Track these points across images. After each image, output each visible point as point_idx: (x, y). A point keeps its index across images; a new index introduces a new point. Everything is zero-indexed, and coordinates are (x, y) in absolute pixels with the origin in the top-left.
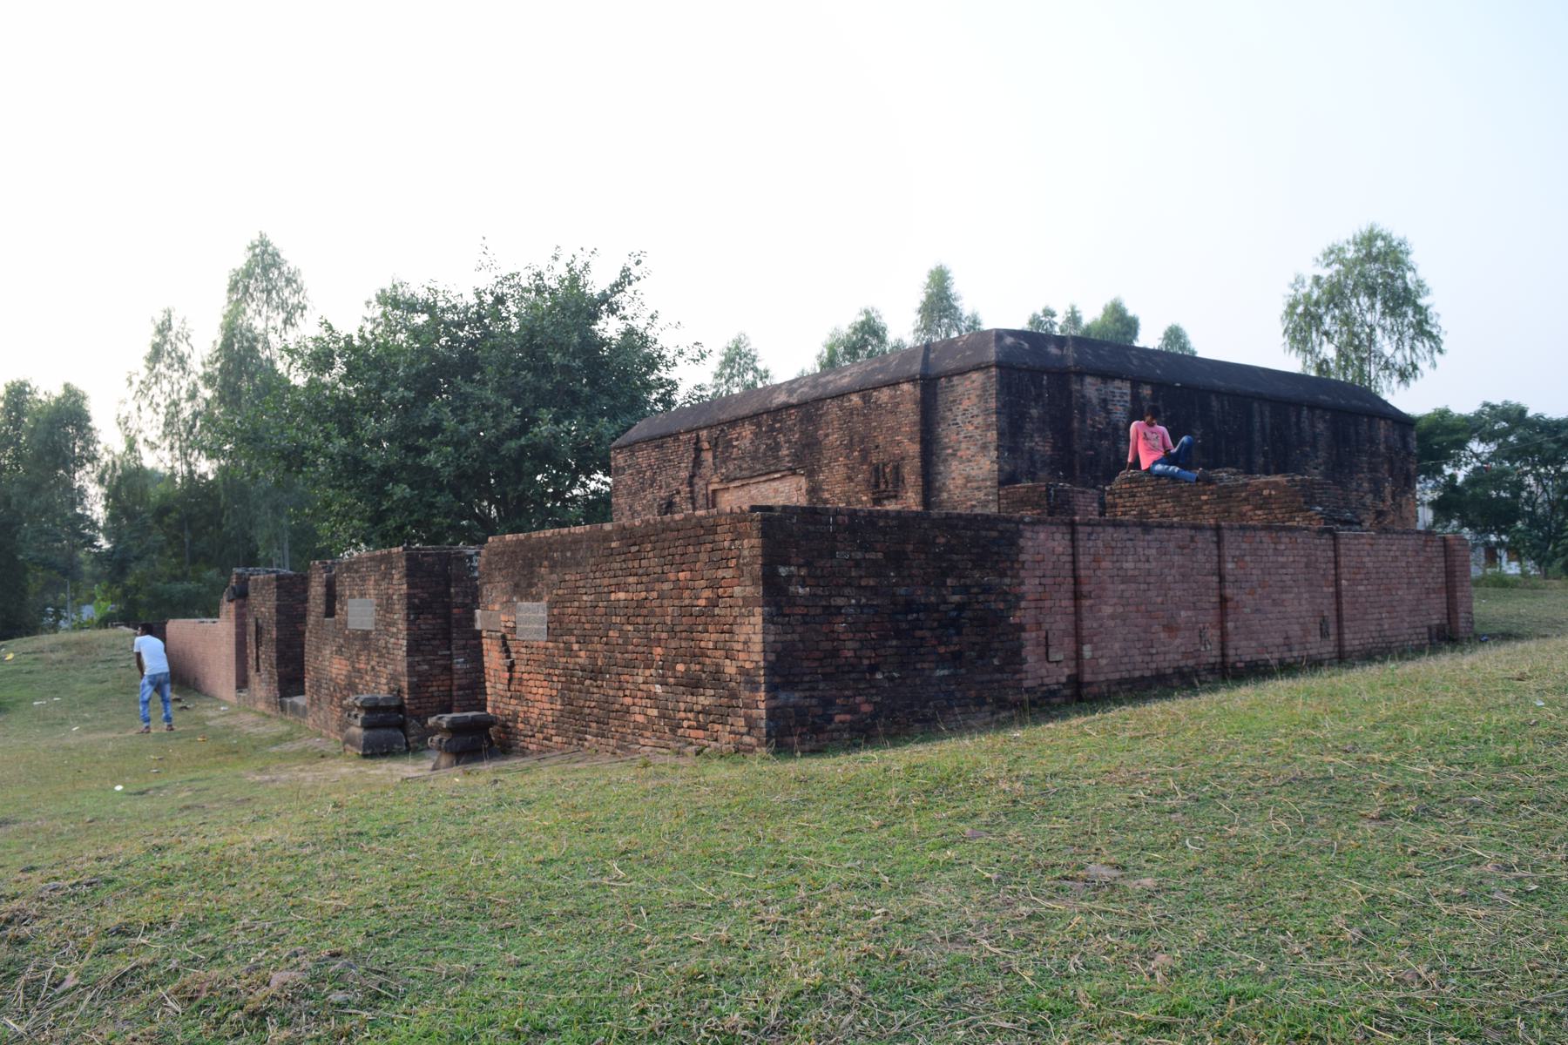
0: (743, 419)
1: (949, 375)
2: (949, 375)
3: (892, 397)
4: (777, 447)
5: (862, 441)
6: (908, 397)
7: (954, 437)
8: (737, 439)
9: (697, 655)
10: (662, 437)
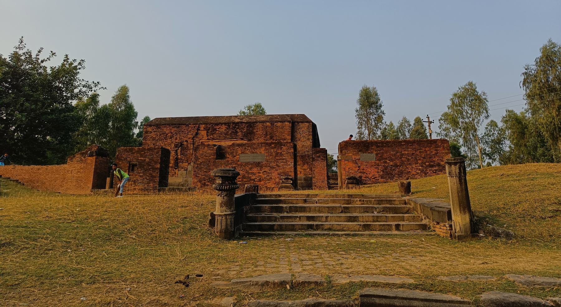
0: (222, 124)
1: (298, 123)
2: (298, 123)
4: (237, 132)
7: (299, 136)
8: (219, 129)
10: (179, 125)
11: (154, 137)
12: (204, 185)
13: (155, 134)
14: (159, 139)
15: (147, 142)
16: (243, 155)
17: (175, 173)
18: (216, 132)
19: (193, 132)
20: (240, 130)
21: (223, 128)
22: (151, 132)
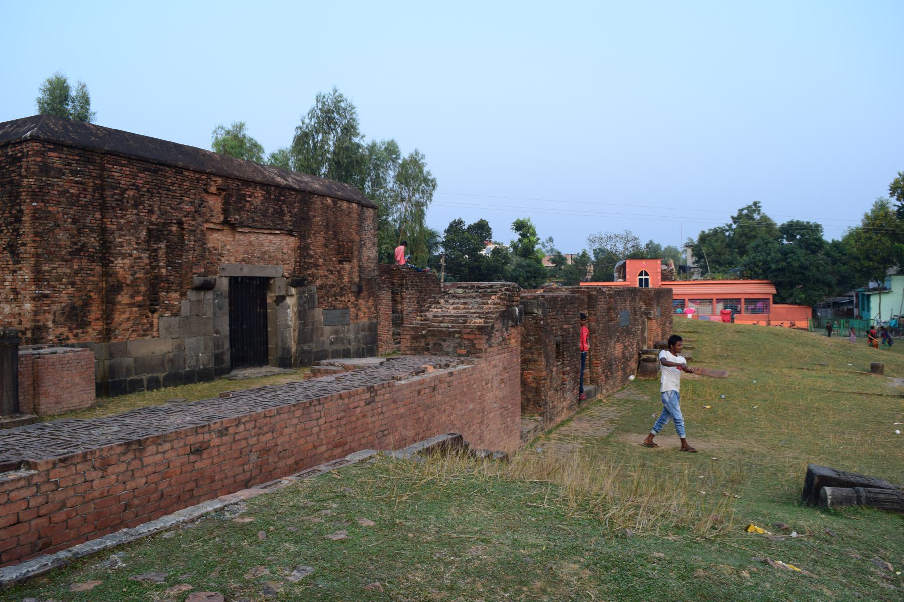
0: (256, 183)
3: (348, 208)
4: (282, 213)
5: (334, 226)
6: (355, 211)
8: (250, 197)
11: (72, 195)
13: (77, 182)
14: (91, 203)
15: (50, 209)
17: (152, 325)
18: (245, 205)
19: (195, 194)
20: (287, 207)
21: (257, 198)
22: (60, 172)
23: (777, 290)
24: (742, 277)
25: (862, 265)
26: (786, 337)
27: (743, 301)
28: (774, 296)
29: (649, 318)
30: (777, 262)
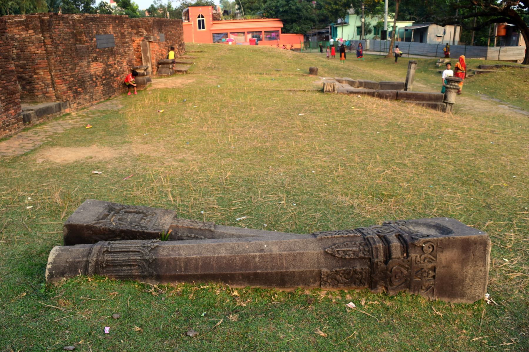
9: (180, 41)
12: (77, 94)
16: (99, 37)
23: (284, 24)
24: (263, 17)
25: (332, 8)
26: (261, 52)
27: (263, 33)
28: (282, 28)
29: (150, 42)
30: (283, 7)
